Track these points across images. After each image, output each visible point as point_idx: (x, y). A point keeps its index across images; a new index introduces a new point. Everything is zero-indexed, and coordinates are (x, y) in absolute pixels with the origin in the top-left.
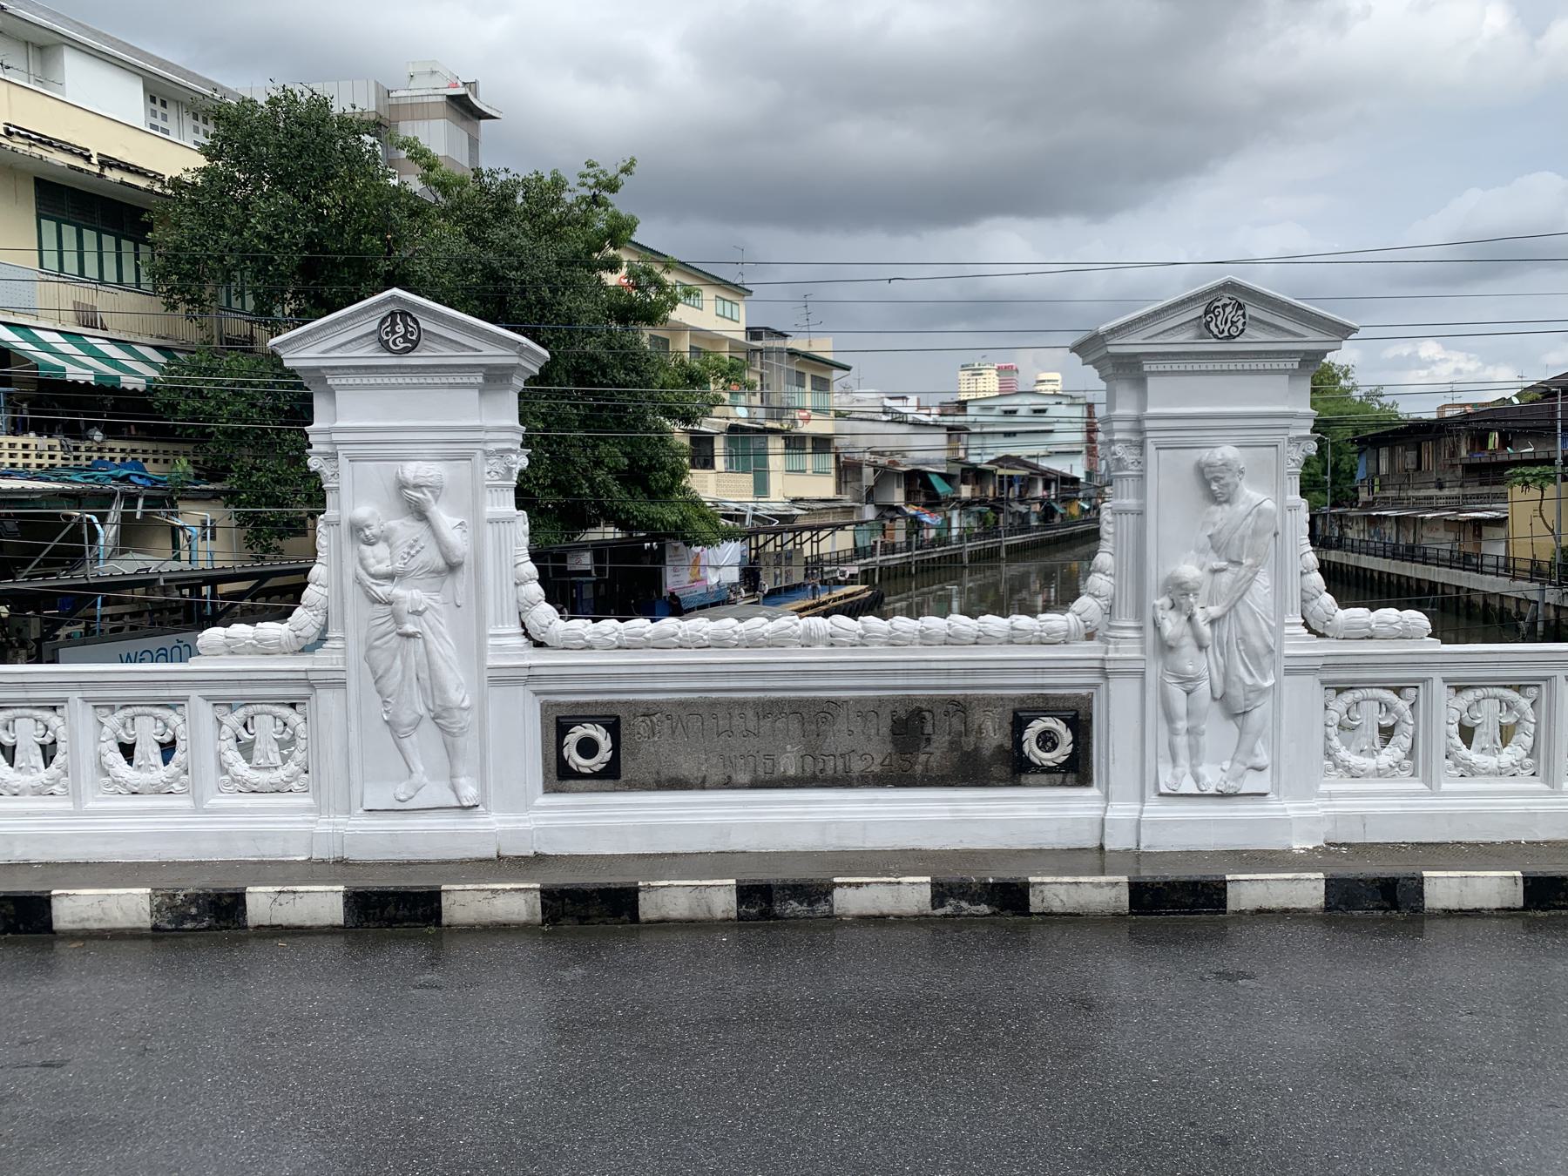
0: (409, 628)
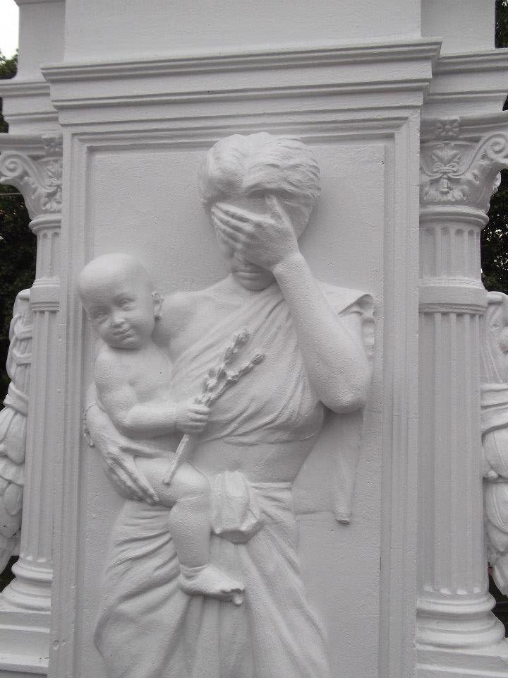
0: (215, 579)
